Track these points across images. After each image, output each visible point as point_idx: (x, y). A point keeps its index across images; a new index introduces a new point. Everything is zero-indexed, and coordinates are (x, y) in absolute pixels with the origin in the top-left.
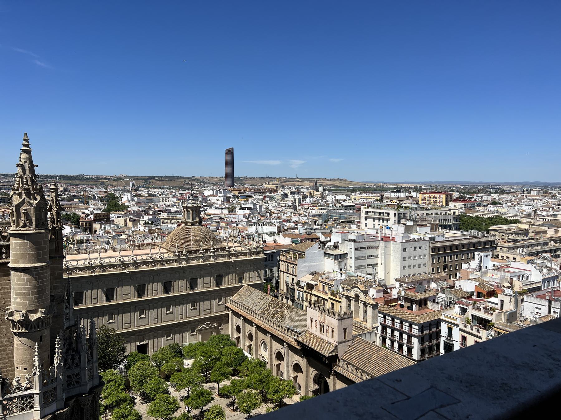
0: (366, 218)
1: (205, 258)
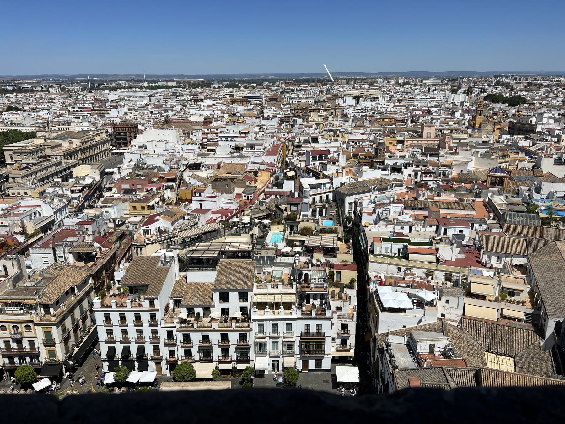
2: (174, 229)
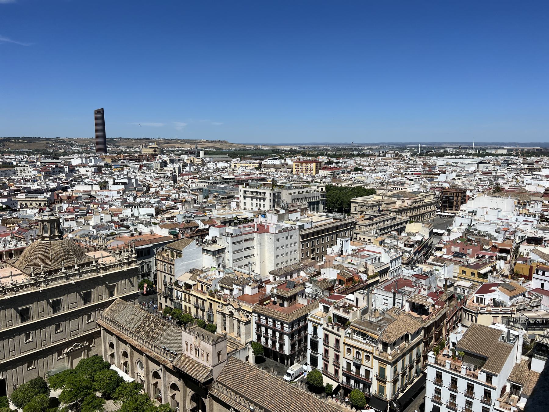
0: (245, 197)
1: (67, 277)
2: (512, 305)
